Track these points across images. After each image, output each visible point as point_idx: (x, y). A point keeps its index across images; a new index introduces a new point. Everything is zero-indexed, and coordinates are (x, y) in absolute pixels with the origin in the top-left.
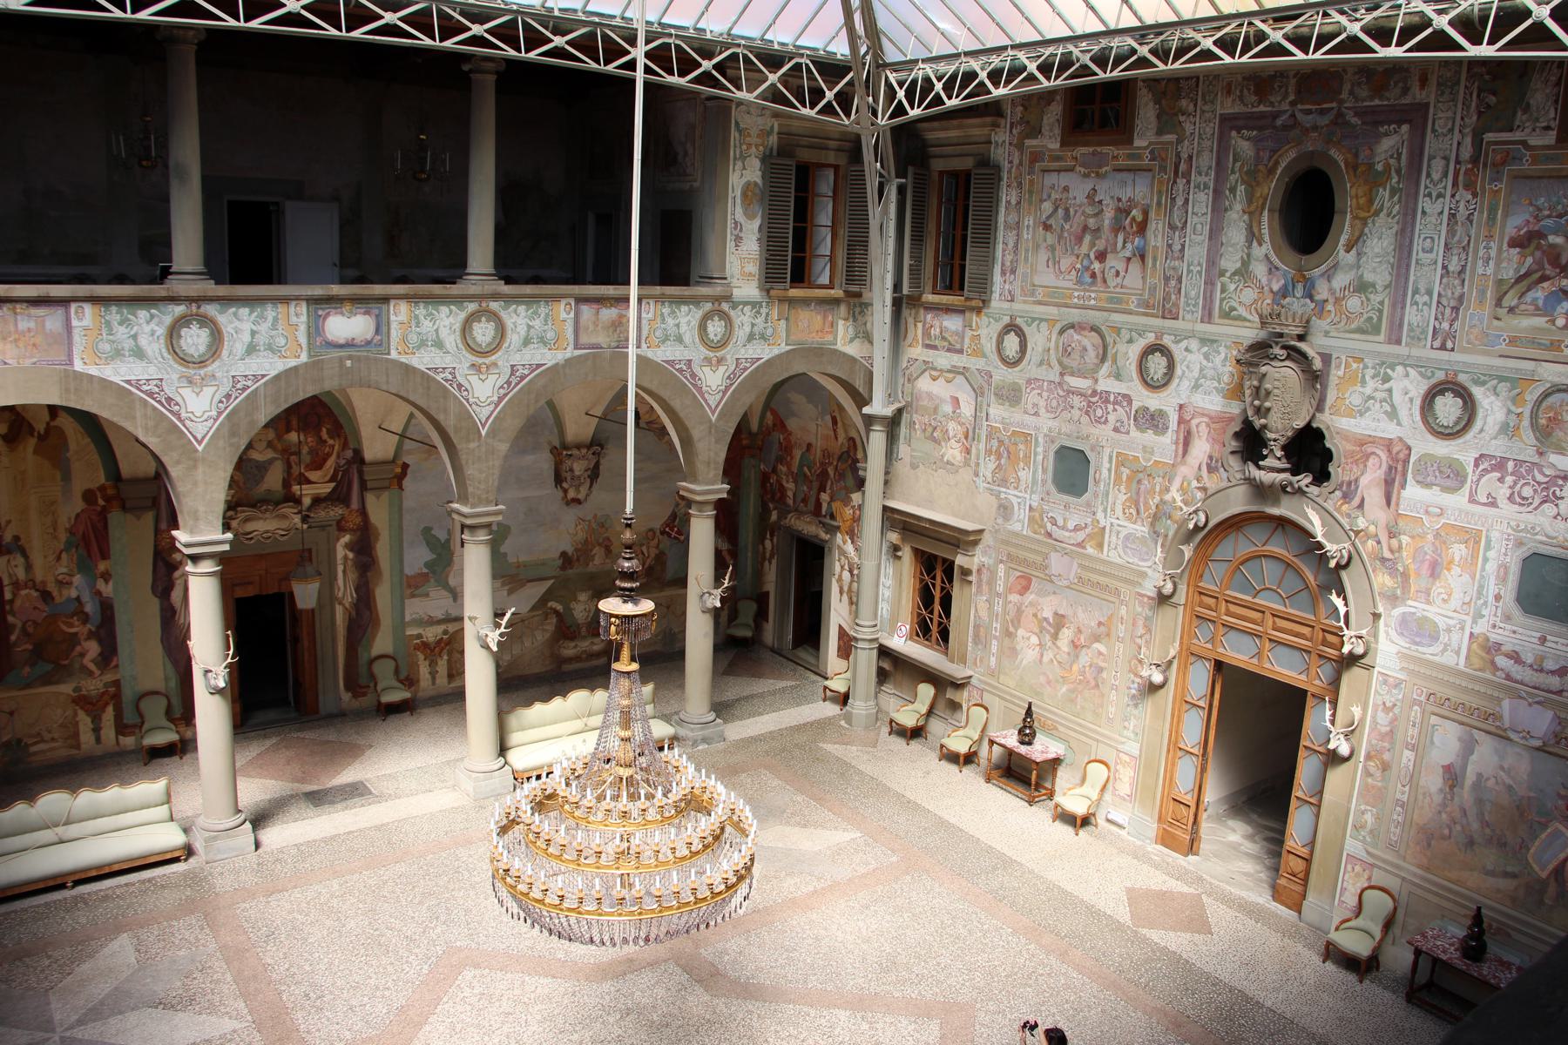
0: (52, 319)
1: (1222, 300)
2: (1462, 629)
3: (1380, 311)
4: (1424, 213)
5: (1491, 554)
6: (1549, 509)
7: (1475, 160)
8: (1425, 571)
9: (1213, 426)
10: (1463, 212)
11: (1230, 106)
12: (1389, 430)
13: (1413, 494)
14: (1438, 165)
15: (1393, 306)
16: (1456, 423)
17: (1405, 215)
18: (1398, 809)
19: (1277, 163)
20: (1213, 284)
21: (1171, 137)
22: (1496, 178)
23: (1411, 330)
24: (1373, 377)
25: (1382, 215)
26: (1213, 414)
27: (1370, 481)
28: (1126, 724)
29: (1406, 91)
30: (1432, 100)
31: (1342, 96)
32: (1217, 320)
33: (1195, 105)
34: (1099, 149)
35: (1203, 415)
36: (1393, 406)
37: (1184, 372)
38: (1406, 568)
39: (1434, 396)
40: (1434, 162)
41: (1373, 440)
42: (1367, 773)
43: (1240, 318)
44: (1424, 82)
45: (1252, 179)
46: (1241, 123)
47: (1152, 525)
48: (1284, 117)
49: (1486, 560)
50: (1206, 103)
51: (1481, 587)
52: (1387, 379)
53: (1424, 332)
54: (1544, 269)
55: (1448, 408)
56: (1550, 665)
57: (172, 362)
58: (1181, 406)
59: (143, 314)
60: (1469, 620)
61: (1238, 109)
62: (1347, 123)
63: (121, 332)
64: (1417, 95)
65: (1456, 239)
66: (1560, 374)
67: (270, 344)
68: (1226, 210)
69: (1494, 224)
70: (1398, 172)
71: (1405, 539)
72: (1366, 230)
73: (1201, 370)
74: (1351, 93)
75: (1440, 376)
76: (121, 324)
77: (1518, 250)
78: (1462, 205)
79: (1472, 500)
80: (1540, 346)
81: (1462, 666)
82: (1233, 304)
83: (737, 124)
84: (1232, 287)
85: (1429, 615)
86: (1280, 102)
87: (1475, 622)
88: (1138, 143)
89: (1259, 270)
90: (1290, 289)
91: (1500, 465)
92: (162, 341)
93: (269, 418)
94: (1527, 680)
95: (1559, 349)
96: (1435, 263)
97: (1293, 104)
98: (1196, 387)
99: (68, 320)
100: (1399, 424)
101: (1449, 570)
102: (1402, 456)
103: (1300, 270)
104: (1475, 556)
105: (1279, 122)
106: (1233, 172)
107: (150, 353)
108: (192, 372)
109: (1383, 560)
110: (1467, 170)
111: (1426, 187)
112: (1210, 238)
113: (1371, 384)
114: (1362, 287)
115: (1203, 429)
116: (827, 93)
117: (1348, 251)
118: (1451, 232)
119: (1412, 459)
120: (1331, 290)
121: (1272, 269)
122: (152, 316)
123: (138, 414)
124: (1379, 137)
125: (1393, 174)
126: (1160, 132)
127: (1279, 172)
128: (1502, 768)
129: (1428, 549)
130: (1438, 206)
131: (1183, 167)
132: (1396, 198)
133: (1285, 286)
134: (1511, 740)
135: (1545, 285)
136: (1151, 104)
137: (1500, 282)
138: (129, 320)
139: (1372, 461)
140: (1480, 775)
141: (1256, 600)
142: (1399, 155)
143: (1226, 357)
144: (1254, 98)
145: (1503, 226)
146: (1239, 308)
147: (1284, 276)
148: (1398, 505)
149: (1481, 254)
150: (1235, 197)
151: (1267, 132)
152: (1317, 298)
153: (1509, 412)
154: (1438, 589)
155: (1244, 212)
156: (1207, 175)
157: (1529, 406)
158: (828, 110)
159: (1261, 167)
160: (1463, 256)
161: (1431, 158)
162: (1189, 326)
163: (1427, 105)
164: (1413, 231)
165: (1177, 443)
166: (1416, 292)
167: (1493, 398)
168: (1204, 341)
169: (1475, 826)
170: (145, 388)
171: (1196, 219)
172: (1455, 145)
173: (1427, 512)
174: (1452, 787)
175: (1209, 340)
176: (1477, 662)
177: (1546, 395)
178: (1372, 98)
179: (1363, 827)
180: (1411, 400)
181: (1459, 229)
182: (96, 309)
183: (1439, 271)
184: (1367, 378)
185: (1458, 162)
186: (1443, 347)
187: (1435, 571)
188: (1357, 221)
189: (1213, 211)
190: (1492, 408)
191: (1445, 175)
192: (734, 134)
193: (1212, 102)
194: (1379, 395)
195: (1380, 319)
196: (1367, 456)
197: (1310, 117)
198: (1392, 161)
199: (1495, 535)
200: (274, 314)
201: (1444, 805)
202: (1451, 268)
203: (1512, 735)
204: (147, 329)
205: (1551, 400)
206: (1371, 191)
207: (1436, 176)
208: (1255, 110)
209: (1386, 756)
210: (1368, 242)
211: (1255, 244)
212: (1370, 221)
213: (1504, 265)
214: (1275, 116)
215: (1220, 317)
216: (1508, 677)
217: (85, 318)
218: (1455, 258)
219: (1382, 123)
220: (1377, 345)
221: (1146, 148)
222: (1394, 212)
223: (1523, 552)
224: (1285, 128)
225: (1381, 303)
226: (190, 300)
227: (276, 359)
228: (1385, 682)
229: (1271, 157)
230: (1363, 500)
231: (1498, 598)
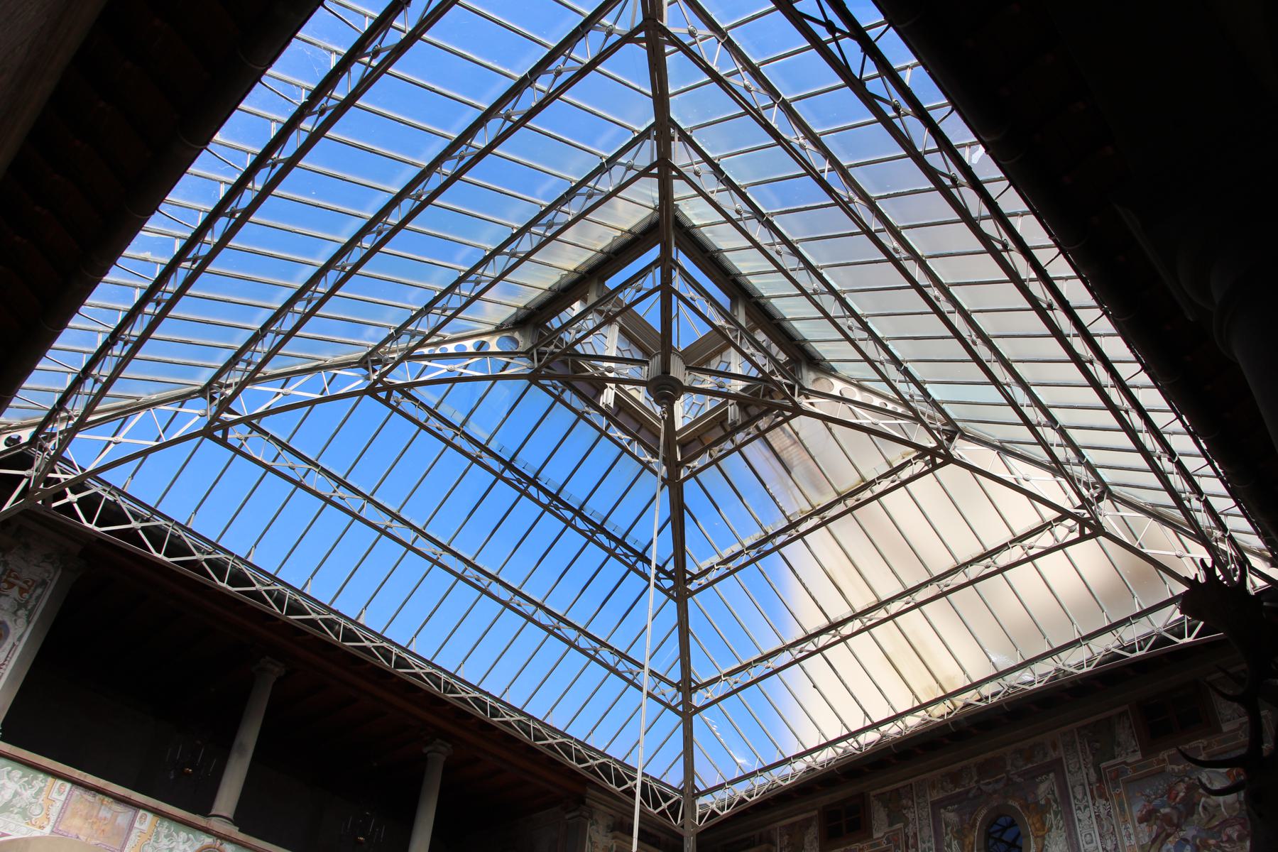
0: (123, 815)
4: (1079, 820)
7: (1100, 780)
10: (1103, 812)
11: (937, 795)
14: (1079, 790)
17: (1068, 825)
19: (975, 820)
21: (899, 825)
22: (1116, 786)
25: (1053, 830)
29: (1045, 755)
31: (1008, 769)
33: (913, 801)
34: (848, 848)
40: (1075, 789)
45: (961, 835)
48: (974, 791)
54: (1165, 829)
59: (183, 835)
61: (942, 795)
63: (164, 842)
64: (1053, 755)
65: (1105, 829)
69: (1125, 812)
70: (1055, 801)
72: (1046, 843)
76: (166, 837)
77: (1145, 824)
83: (590, 837)
86: (969, 783)
88: (875, 837)
96: (1097, 848)
97: (977, 782)
99: (133, 821)
105: (971, 795)
106: (947, 834)
110: (1097, 787)
111: (1076, 804)
116: (663, 804)
118: (1100, 826)
122: (189, 839)
125: (1053, 803)
126: (891, 825)
127: (978, 824)
130: (1087, 812)
131: (911, 841)
132: (1059, 817)
135: (1171, 839)
136: (882, 809)
142: (1053, 791)
144: (951, 786)
145: (1131, 815)
149: (1124, 834)
156: (929, 842)
158: (663, 813)
159: (966, 826)
160: (1113, 838)
163: (1061, 758)
164: (1076, 834)
172: (1085, 776)
178: (1026, 765)
181: (1104, 822)
182: (156, 818)
185: (1090, 784)
191: (1085, 794)
192: (588, 843)
197: (990, 786)
198: (1049, 796)
204: (182, 847)
206: (1042, 818)
207: (1079, 797)
208: (953, 792)
212: (1047, 836)
213: (1141, 835)
214: (967, 792)
217: (146, 822)
218: (1109, 842)
221: (883, 837)
222: (1061, 825)
226: (218, 836)
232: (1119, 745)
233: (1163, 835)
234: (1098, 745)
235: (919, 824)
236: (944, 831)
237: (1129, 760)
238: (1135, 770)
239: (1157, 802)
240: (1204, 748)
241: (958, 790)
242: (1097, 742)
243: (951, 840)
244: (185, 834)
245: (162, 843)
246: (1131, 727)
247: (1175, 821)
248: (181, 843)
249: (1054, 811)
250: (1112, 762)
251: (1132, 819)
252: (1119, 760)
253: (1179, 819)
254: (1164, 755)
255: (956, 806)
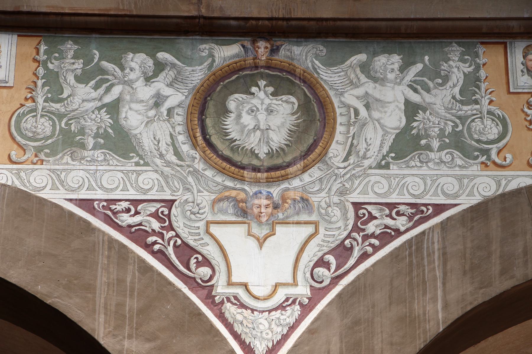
57: (200, 166)
67: (456, 135)
92: (179, 119)
93: (456, 313)
107: (147, 143)
108: (251, 190)
122: (160, 67)
123: (102, 279)
138: (103, 71)
170: (126, 219)
200: (467, 69)
227: (475, 169)
244: (141, 57)
245: (77, 100)
248: (140, 84)
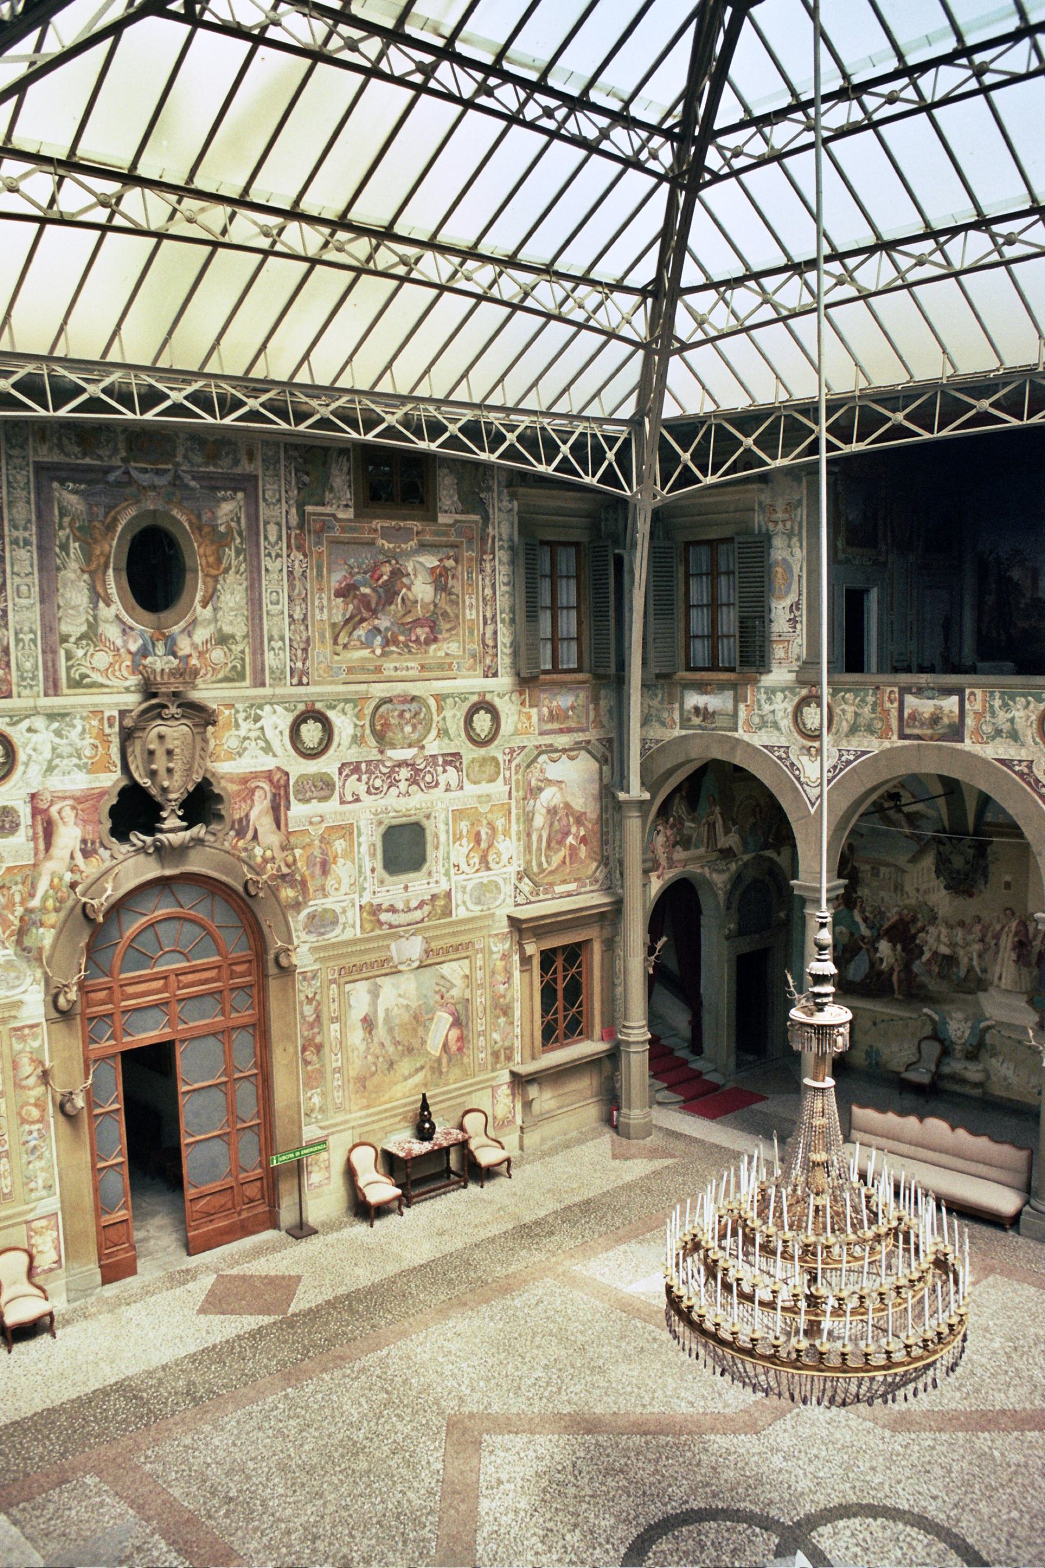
1: (69, 669)
2: (353, 905)
3: (243, 660)
4: (267, 570)
5: (363, 839)
6: (394, 791)
7: (301, 526)
8: (318, 870)
9: (80, 807)
11: (47, 455)
12: (268, 763)
13: (298, 811)
14: (272, 531)
15: (254, 653)
16: (320, 744)
17: (251, 572)
18: (337, 1075)
19: (115, 520)
20: (54, 652)
23: (272, 672)
24: (245, 719)
26: (78, 794)
27: (259, 813)
28: (32, 1185)
29: (236, 462)
30: (260, 473)
32: (66, 691)
35: (65, 798)
36: (267, 741)
37: (30, 756)
38: (303, 876)
39: (299, 725)
41: (255, 776)
42: (306, 1063)
43: (94, 685)
44: (251, 456)
45: (87, 535)
46: (64, 474)
47: (19, 942)
48: (118, 473)
49: (359, 844)
50: (12, 447)
51: (360, 867)
52: (257, 719)
53: (283, 672)
54: (360, 612)
55: (311, 733)
56: (414, 904)
58: (33, 796)
60: (356, 896)
61: (56, 458)
62: (187, 486)
64: (246, 467)
66: (383, 691)
68: (58, 569)
70: (240, 534)
71: (298, 852)
72: (219, 587)
73: (54, 749)
74: (185, 457)
75: (301, 707)
78: (297, 563)
79: (342, 802)
80: (368, 671)
81: (359, 935)
82: (83, 670)
84: (80, 653)
85: (328, 906)
86: (110, 457)
87: (361, 896)
89: (112, 632)
90: (150, 648)
91: (356, 769)
94: (402, 922)
95: (380, 672)
97: (124, 460)
98: (50, 769)
100: (275, 756)
101: (335, 863)
102: (282, 782)
103: (158, 628)
104: (351, 845)
105: (112, 477)
106: (61, 527)
109: (283, 877)
112: (42, 601)
113: (245, 726)
114: (223, 639)
115: (69, 814)
117: (204, 607)
118: (292, 587)
119: (291, 783)
120: (194, 646)
121: (126, 630)
124: (220, 501)
127: (119, 529)
128: (400, 996)
129: (317, 852)
130: (278, 564)
132: (241, 558)
133: (144, 646)
134: (400, 972)
135: (364, 625)
137: (334, 625)
139: (258, 794)
140: (387, 1010)
141: (155, 970)
142: (239, 519)
143: (84, 731)
144: (76, 449)
145: (329, 582)
146: (93, 675)
147: (142, 636)
148: (287, 825)
149: (317, 604)
150: (68, 555)
151: (99, 487)
152: (180, 653)
153: (356, 726)
154: (330, 882)
155: (83, 571)
156: (25, 529)
157: (368, 718)
159: (97, 524)
161: (266, 523)
162: (30, 703)
163: (256, 477)
165: (35, 839)
166: (271, 639)
167: (343, 717)
168: (51, 717)
169: (391, 1049)
171: (17, 580)
173: (311, 823)
174: (370, 1033)
175: (59, 715)
176: (368, 926)
177: (377, 707)
178: (207, 464)
179: (312, 1111)
180: (281, 733)
181: (297, 583)
183: (287, 620)
184: (240, 721)
185: (288, 528)
186: (300, 683)
187: (325, 868)
188: (209, 579)
189: (40, 570)
190: (343, 724)
191: (280, 538)
193: (22, 447)
194: (253, 735)
195: (243, 667)
196: (252, 792)
198: (233, 524)
199: (362, 824)
201: (368, 1049)
202: (296, 617)
203: (401, 968)
205: (381, 710)
207: (273, 538)
208: (78, 461)
209: (318, 1039)
210: (222, 598)
211: (101, 604)
212: (220, 578)
215: (69, 687)
216: (391, 926)
218: (298, 608)
219: (219, 489)
220: (245, 690)
223: (382, 829)
224: (118, 484)
225: (243, 652)
228: (305, 979)
229: (107, 514)
230: (256, 831)
231: (373, 870)
232: (331, 490)
233: (357, 619)
234: (306, 479)
235: (9, 492)
236: (57, 519)
237: (341, 515)
238: (343, 530)
239: (359, 577)
240: (418, 533)
241: (88, 461)
242: (307, 474)
243: (68, 538)
246: (348, 473)
247: (373, 606)
249: (236, 548)
250: (319, 509)
251: (329, 590)
252: (328, 510)
253: (377, 604)
254: (378, 524)
255: (83, 486)
